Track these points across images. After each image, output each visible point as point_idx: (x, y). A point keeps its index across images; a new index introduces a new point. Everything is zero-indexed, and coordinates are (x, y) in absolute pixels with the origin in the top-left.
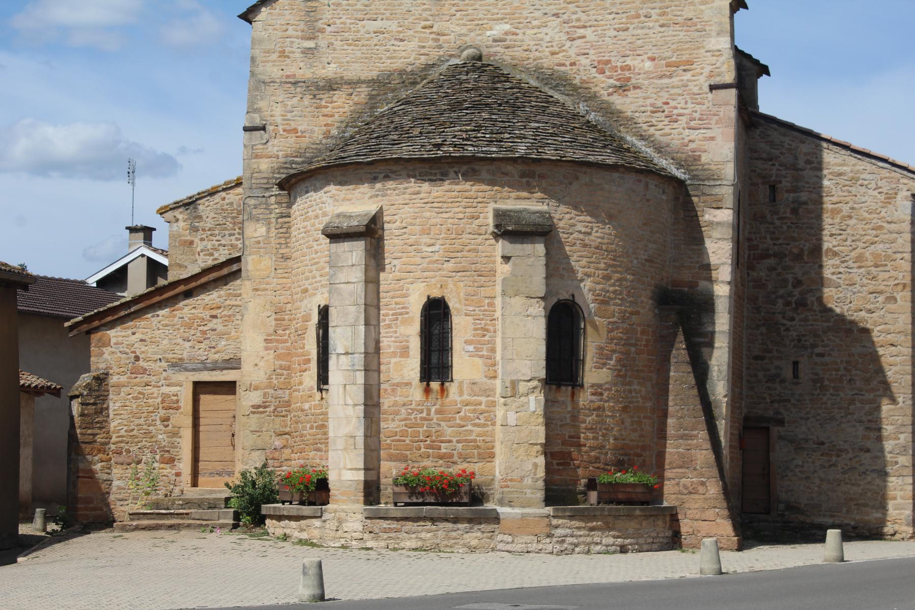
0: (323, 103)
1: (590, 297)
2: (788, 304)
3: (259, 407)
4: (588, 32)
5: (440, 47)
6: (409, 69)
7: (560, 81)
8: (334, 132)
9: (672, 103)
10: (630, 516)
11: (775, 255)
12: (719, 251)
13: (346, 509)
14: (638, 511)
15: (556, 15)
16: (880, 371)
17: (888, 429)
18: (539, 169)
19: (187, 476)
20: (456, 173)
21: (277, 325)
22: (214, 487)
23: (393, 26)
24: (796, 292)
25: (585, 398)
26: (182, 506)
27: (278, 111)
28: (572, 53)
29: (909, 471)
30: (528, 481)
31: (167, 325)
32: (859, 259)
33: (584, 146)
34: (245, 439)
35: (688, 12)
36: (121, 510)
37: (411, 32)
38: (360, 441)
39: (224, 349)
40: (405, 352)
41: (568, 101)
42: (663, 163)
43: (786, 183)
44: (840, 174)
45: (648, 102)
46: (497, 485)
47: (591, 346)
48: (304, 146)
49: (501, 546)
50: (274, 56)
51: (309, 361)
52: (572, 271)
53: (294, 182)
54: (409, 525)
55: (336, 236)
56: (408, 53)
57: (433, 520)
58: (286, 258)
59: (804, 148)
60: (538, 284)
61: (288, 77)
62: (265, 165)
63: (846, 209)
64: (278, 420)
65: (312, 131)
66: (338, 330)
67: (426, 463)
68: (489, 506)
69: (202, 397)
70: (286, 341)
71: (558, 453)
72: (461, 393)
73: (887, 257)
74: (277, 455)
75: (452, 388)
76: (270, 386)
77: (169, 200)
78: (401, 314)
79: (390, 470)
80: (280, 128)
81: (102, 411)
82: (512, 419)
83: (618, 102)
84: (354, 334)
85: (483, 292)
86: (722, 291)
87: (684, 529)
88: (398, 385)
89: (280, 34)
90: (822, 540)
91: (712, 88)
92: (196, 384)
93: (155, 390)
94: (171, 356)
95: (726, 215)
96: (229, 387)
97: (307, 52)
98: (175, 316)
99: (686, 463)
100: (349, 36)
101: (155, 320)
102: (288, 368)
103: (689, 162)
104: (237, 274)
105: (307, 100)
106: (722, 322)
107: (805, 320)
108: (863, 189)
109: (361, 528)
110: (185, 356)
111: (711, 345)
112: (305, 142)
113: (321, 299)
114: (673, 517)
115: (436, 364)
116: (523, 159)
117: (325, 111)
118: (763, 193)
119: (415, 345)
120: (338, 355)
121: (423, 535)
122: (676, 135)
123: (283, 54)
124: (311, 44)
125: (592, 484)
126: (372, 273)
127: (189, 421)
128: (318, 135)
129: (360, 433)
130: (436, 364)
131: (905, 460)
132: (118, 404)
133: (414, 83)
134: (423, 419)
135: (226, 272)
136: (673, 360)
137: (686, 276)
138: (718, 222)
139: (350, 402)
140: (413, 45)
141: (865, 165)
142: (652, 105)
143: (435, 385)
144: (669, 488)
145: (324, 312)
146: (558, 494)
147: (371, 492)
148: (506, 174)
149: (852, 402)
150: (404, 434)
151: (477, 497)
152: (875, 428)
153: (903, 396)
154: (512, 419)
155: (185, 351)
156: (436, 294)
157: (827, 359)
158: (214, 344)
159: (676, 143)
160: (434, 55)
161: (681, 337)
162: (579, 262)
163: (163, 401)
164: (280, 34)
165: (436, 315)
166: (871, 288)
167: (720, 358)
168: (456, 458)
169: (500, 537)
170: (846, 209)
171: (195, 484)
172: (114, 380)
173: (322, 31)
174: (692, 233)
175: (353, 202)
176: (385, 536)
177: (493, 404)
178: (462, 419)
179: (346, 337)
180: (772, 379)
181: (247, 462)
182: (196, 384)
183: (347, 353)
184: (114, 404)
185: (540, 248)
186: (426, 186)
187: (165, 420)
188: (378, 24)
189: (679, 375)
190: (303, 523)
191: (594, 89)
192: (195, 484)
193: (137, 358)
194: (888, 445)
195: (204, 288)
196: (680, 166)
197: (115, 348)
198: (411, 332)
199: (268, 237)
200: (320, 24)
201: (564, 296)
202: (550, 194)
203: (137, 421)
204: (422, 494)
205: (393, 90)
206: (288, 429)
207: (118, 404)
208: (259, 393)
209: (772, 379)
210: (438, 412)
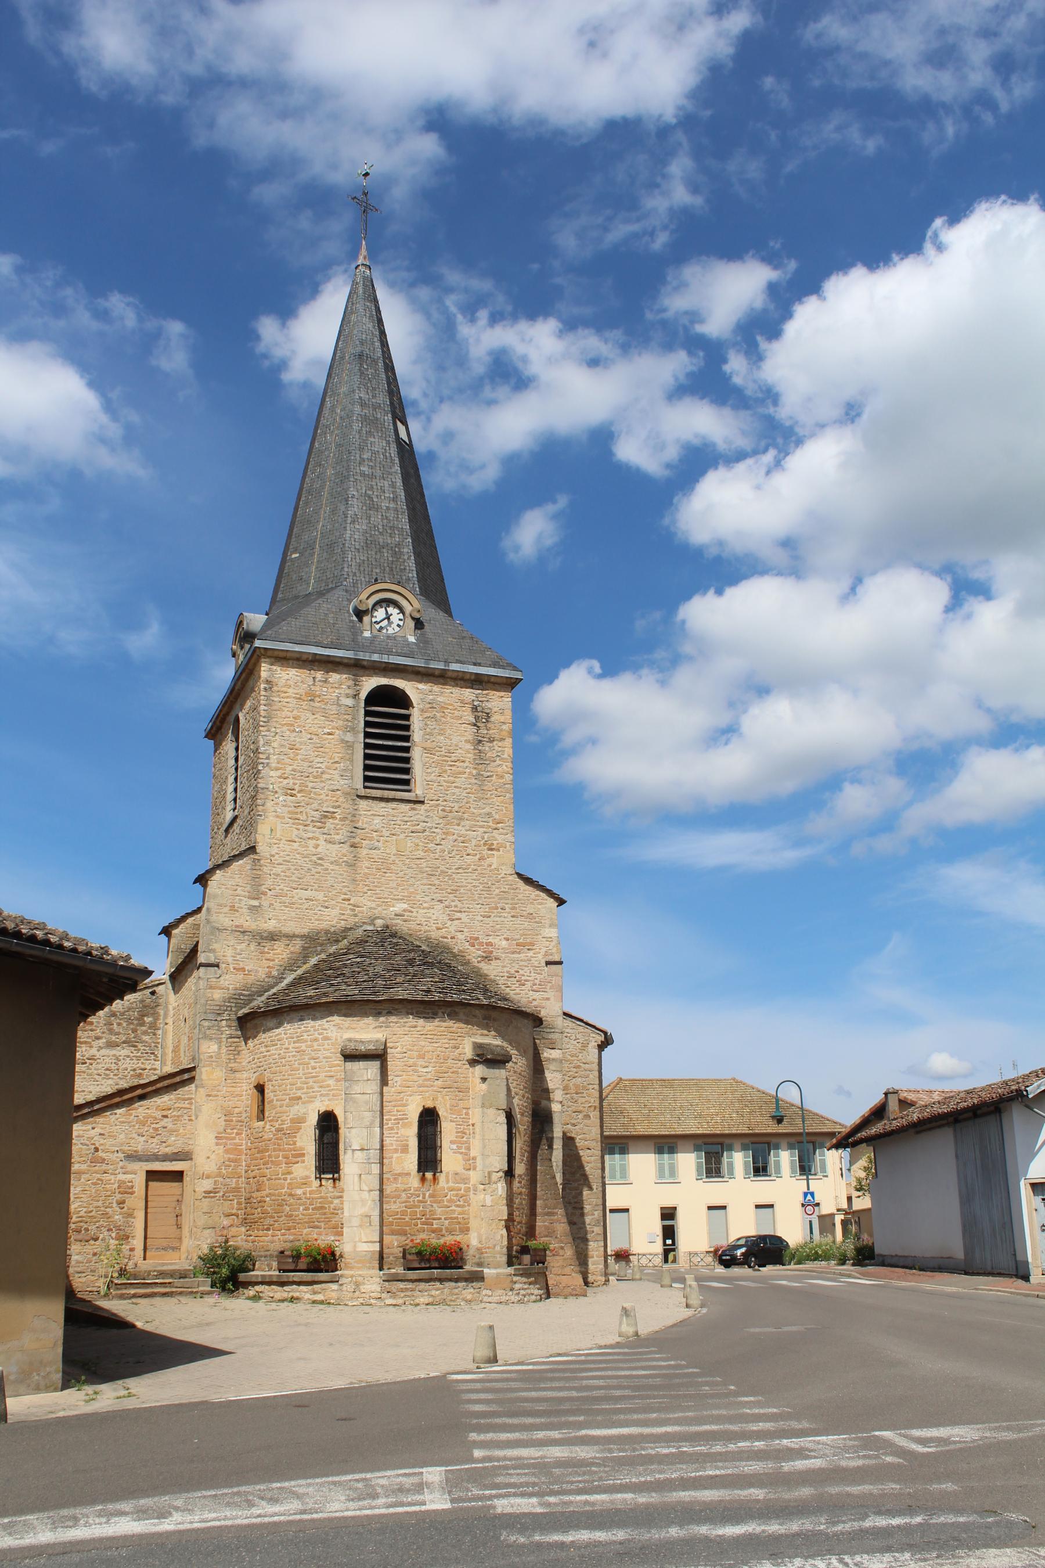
0: (266, 950)
3: (210, 1192)
5: (356, 915)
6: (332, 929)
7: (447, 949)
8: (275, 973)
9: (521, 972)
18: (494, 1014)
19: (139, 1251)
20: (443, 1013)
21: (226, 1126)
23: (320, 896)
26: (157, 1277)
27: (229, 952)
30: (498, 1248)
31: (123, 1122)
37: (334, 902)
40: (405, 1149)
45: (505, 969)
46: (471, 1252)
48: (250, 982)
55: (350, 1056)
56: (332, 918)
61: (237, 926)
62: (218, 995)
65: (257, 971)
66: (354, 1131)
69: (150, 1183)
70: (234, 1138)
72: (448, 1182)
73: (584, 1087)
75: (442, 1177)
76: (220, 1175)
78: (402, 1119)
80: (231, 966)
85: (461, 1104)
88: (399, 1175)
89: (232, 892)
91: (548, 963)
92: (147, 1172)
93: (112, 1177)
94: (126, 1148)
96: (178, 1176)
97: (253, 909)
98: (131, 1115)
100: (287, 900)
101: (113, 1118)
104: (192, 1080)
105: (253, 946)
108: (567, 1040)
109: (379, 1289)
110: (140, 1148)
112: (251, 979)
115: (429, 1160)
117: (268, 956)
119: (413, 1144)
120: (353, 1150)
121: (433, 1293)
123: (233, 909)
124: (256, 903)
128: (262, 974)
130: (429, 1160)
132: (79, 1189)
133: (337, 941)
134: (419, 1201)
135: (181, 1078)
136: (539, 1158)
139: (365, 1188)
140: (336, 912)
142: (508, 972)
143: (429, 1175)
148: (475, 1016)
150: (404, 1213)
155: (140, 1145)
156: (430, 1104)
158: (164, 1139)
160: (352, 921)
163: (119, 1187)
164: (232, 892)
165: (429, 1119)
166: (574, 1108)
168: (444, 1232)
169: (485, 1292)
173: (265, 894)
176: (402, 1295)
178: (448, 1201)
182: (147, 1172)
183: (362, 1149)
186: (421, 1021)
187: (121, 1203)
191: (468, 957)
193: (97, 1150)
195: (157, 1092)
198: (411, 1133)
199: (219, 1053)
200: (263, 888)
203: (96, 1204)
204: (429, 1260)
205: (321, 945)
206: (234, 1211)
207: (79, 1189)
208: (211, 1181)
210: (431, 1196)
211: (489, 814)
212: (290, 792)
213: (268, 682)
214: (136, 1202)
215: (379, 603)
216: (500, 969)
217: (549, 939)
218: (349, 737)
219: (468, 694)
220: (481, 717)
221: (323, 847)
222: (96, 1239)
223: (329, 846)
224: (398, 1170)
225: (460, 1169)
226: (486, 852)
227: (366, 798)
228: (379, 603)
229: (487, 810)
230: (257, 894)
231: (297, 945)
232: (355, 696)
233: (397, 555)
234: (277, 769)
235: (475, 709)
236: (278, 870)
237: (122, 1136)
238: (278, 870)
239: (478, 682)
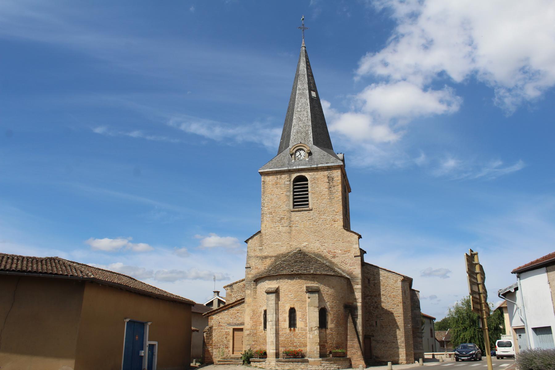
1: (329, 307)
10: (340, 360)
12: (358, 295)
13: (271, 360)
14: (342, 359)
16: (396, 323)
17: (399, 337)
18: (316, 276)
19: (231, 352)
22: (238, 354)
23: (280, 243)
25: (328, 331)
27: (253, 263)
28: (322, 249)
29: (404, 347)
30: (315, 352)
32: (390, 296)
33: (326, 271)
34: (245, 342)
35: (349, 239)
36: (215, 360)
38: (274, 342)
41: (321, 260)
42: (344, 274)
43: (372, 279)
47: (330, 318)
52: (324, 300)
53: (257, 280)
54: (287, 363)
55: (268, 293)
56: (284, 250)
57: (293, 362)
58: (255, 298)
59: (376, 270)
60: (316, 303)
62: (250, 276)
63: (386, 284)
67: (291, 348)
68: (306, 358)
71: (322, 345)
75: (297, 329)
76: (251, 329)
77: (226, 285)
78: (285, 311)
79: (282, 350)
81: (211, 335)
82: (311, 336)
83: (333, 260)
84: (273, 316)
85: (303, 306)
86: (359, 304)
87: (353, 363)
90: (387, 365)
91: (355, 257)
92: (234, 329)
95: (359, 286)
96: (241, 330)
97: (260, 250)
99: (353, 347)
103: (350, 274)
105: (260, 261)
106: (360, 312)
111: (357, 318)
112: (260, 271)
113: (264, 308)
114: (350, 360)
115: (292, 323)
116: (312, 274)
118: (367, 281)
119: (287, 319)
122: (347, 268)
125: (330, 353)
127: (232, 338)
128: (263, 269)
129: (275, 341)
130: (292, 323)
131: (403, 345)
135: (241, 302)
137: (351, 301)
138: (358, 288)
140: (285, 248)
141: (390, 274)
143: (292, 329)
144: (349, 353)
145: (265, 311)
146: (322, 355)
147: (277, 355)
149: (390, 331)
150: (285, 341)
151: (303, 356)
152: (395, 337)
153: (402, 329)
154: (311, 336)
155: (231, 321)
156: (292, 306)
159: (347, 270)
160: (290, 250)
161: (350, 316)
162: (326, 298)
165: (292, 311)
167: (359, 321)
170: (386, 284)
171: (233, 353)
172: (214, 328)
174: (352, 291)
175: (272, 285)
177: (306, 333)
179: (271, 317)
180: (371, 326)
181: (246, 348)
182: (234, 329)
184: (214, 334)
185: (317, 295)
186: (289, 281)
187: (226, 338)
188: (277, 243)
189: (350, 325)
192: (233, 353)
194: (399, 341)
195: (236, 306)
196: (348, 275)
197: (214, 320)
201: (323, 306)
202: (319, 283)
209: (371, 326)
211: (334, 210)
213: (264, 181)
217: (356, 248)
218: (288, 194)
219: (326, 173)
220: (330, 179)
226: (333, 223)
230: (261, 245)
231: (274, 258)
232: (290, 181)
235: (328, 177)
236: (267, 237)
238: (267, 237)
239: (329, 168)
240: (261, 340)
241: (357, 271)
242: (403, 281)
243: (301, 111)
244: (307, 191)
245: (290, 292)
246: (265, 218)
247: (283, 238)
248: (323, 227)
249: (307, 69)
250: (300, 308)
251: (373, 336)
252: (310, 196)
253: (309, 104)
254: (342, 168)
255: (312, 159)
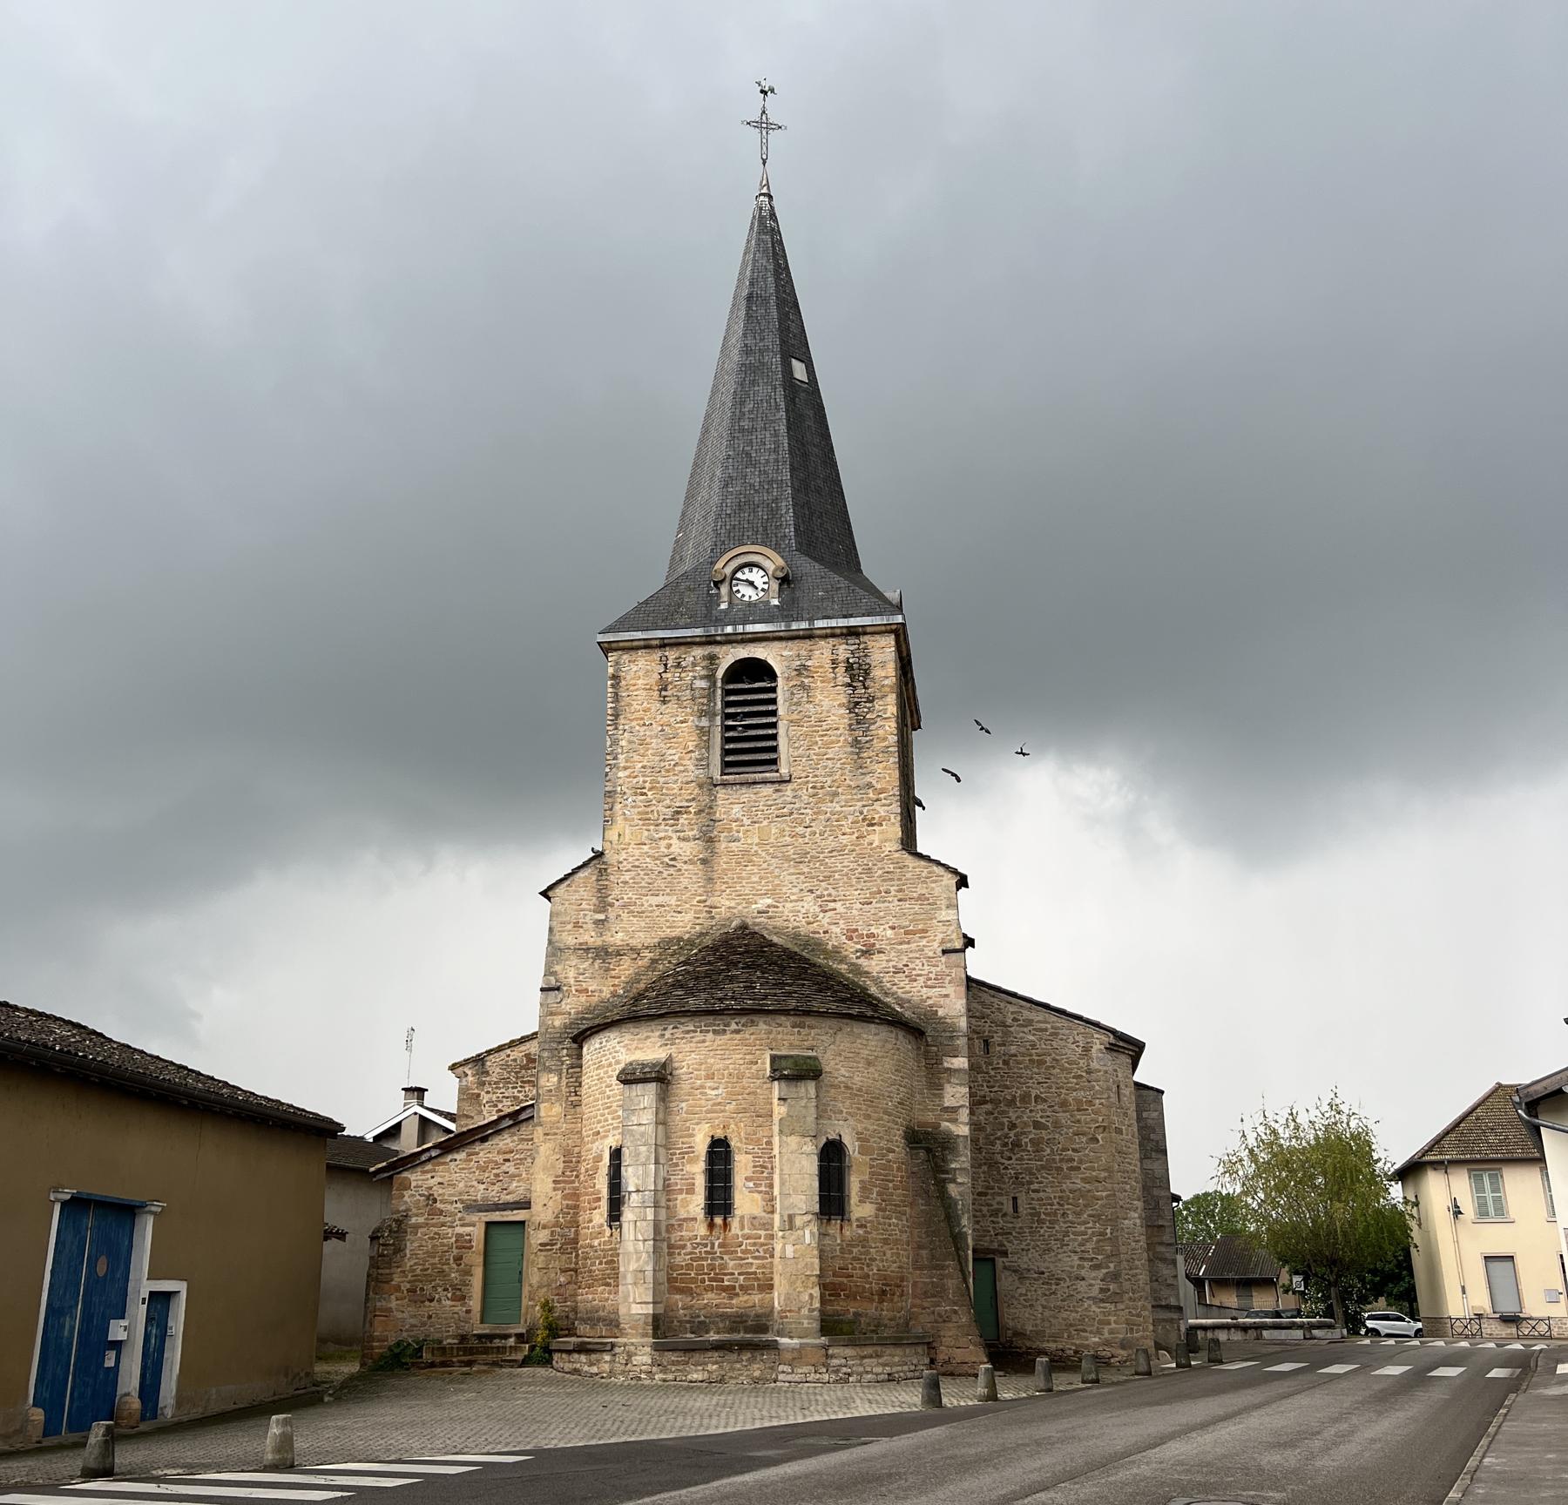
2: (1005, 1145)
4: (838, 905)
6: (686, 937)
7: (817, 946)
11: (991, 1101)
15: (811, 891)
23: (673, 900)
24: (1012, 1134)
27: (572, 974)
30: (805, 1311)
35: (921, 889)
38: (649, 1275)
39: (517, 1191)
40: (691, 1190)
43: (997, 1038)
44: (1041, 1030)
49: (781, 1377)
50: (569, 927)
51: (599, 1199)
55: (629, 1078)
62: (558, 1022)
64: (564, 1257)
66: (630, 1169)
72: (742, 1228)
74: (562, 1290)
75: (735, 1224)
76: (557, 1224)
84: (646, 1174)
88: (685, 1220)
91: (944, 952)
92: (488, 1224)
97: (597, 922)
102: (576, 1207)
107: (1021, 1159)
113: (612, 1141)
115: (719, 1202)
119: (700, 1182)
123: (577, 925)
124: (602, 917)
126: (661, 1116)
128: (606, 994)
129: (650, 1267)
130: (719, 1202)
135: (518, 1118)
137: (930, 1117)
140: (689, 916)
141: (1061, 1022)
143: (718, 1220)
145: (616, 1154)
146: (830, 1326)
149: (1066, 1234)
150: (689, 1267)
155: (479, 1193)
156: (719, 1134)
157: (1041, 1194)
165: (720, 1153)
169: (781, 1368)
173: (612, 905)
178: (743, 1252)
180: (995, 1213)
187: (458, 1259)
188: (659, 900)
190: (594, 1357)
193: (435, 1201)
198: (697, 1170)
199: (558, 1088)
203: (432, 1261)
208: (547, 1232)
209: (995, 1213)
210: (720, 1246)
212: (640, 791)
214: (475, 1259)
215: (740, 568)
216: (884, 964)
218: (704, 722)
221: (677, 847)
222: (431, 1300)
223: (683, 844)
224: (682, 1214)
225: (758, 1211)
227: (724, 784)
228: (740, 568)
229: (868, 779)
230: (603, 905)
233: (774, 513)
234: (625, 768)
235: (849, 667)
236: (627, 877)
237: (461, 1185)
238: (627, 877)
240: (598, 1268)
241: (953, 1006)
242: (1111, 1048)
243: (753, 430)
244: (774, 713)
245: (710, 1077)
246: (618, 807)
247: (685, 882)
248: (831, 843)
249: (777, 274)
250: (748, 1140)
251: (1005, 1254)
252: (781, 730)
253: (783, 405)
254: (900, 634)
255: (794, 600)
